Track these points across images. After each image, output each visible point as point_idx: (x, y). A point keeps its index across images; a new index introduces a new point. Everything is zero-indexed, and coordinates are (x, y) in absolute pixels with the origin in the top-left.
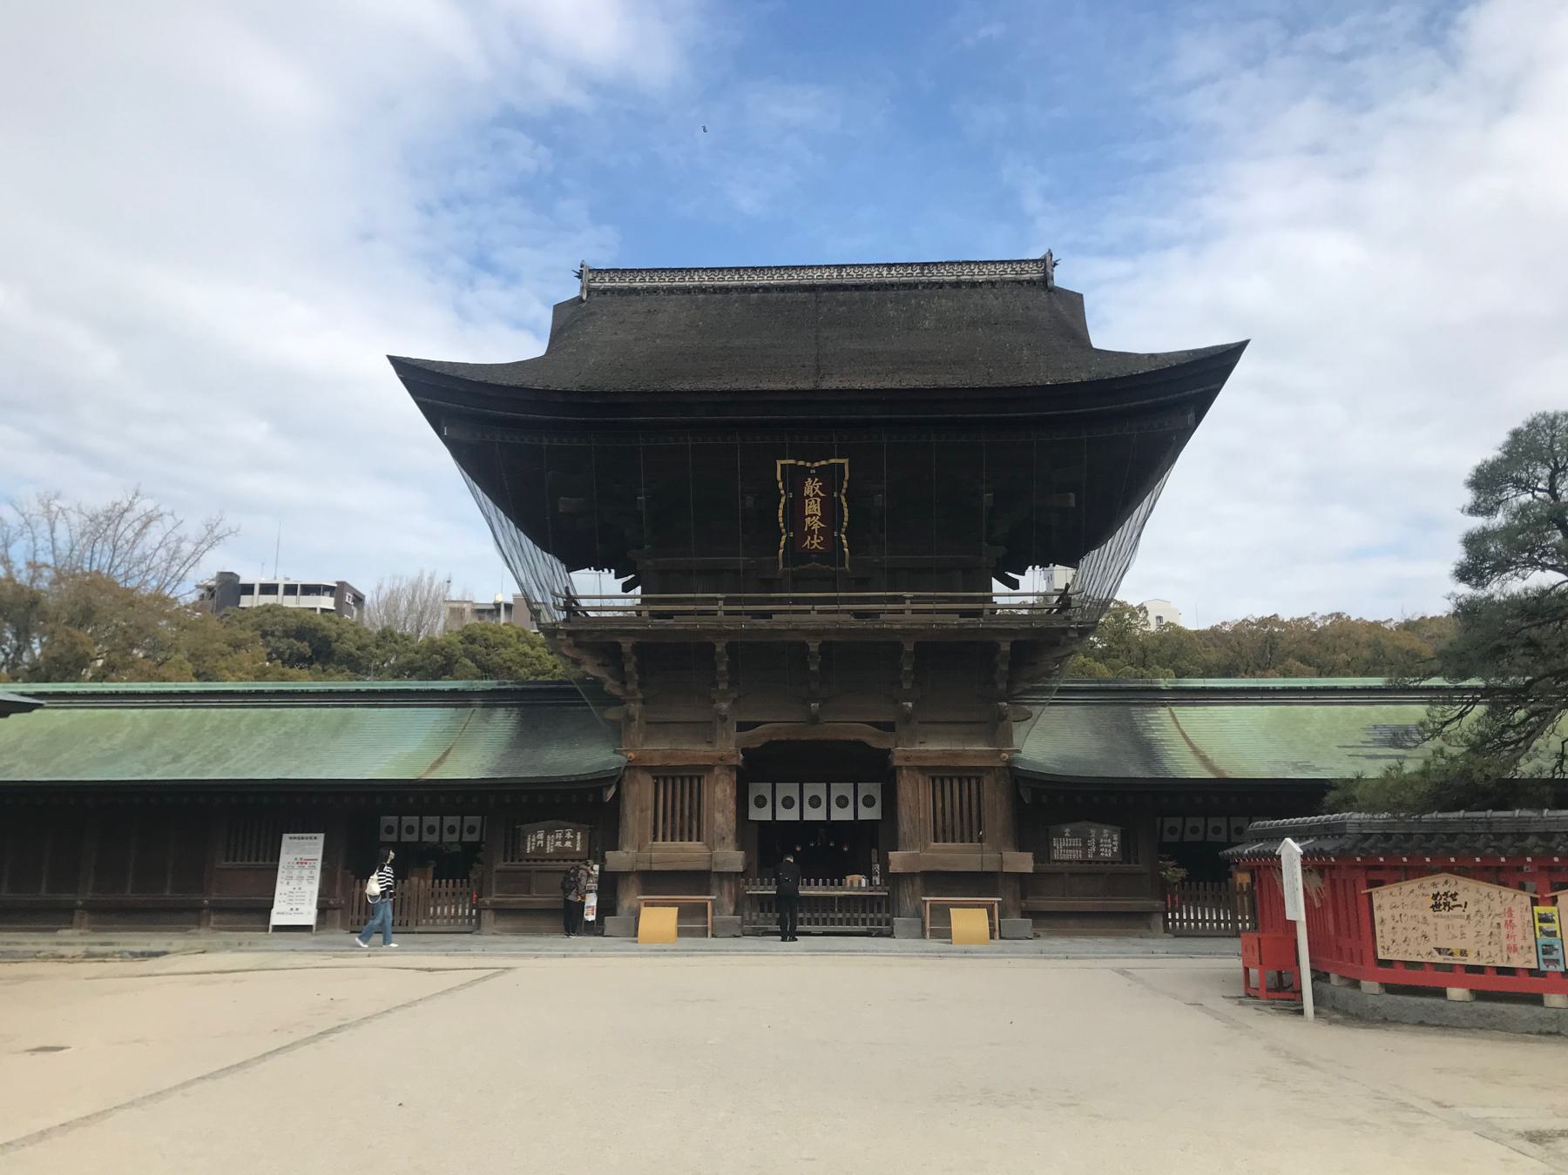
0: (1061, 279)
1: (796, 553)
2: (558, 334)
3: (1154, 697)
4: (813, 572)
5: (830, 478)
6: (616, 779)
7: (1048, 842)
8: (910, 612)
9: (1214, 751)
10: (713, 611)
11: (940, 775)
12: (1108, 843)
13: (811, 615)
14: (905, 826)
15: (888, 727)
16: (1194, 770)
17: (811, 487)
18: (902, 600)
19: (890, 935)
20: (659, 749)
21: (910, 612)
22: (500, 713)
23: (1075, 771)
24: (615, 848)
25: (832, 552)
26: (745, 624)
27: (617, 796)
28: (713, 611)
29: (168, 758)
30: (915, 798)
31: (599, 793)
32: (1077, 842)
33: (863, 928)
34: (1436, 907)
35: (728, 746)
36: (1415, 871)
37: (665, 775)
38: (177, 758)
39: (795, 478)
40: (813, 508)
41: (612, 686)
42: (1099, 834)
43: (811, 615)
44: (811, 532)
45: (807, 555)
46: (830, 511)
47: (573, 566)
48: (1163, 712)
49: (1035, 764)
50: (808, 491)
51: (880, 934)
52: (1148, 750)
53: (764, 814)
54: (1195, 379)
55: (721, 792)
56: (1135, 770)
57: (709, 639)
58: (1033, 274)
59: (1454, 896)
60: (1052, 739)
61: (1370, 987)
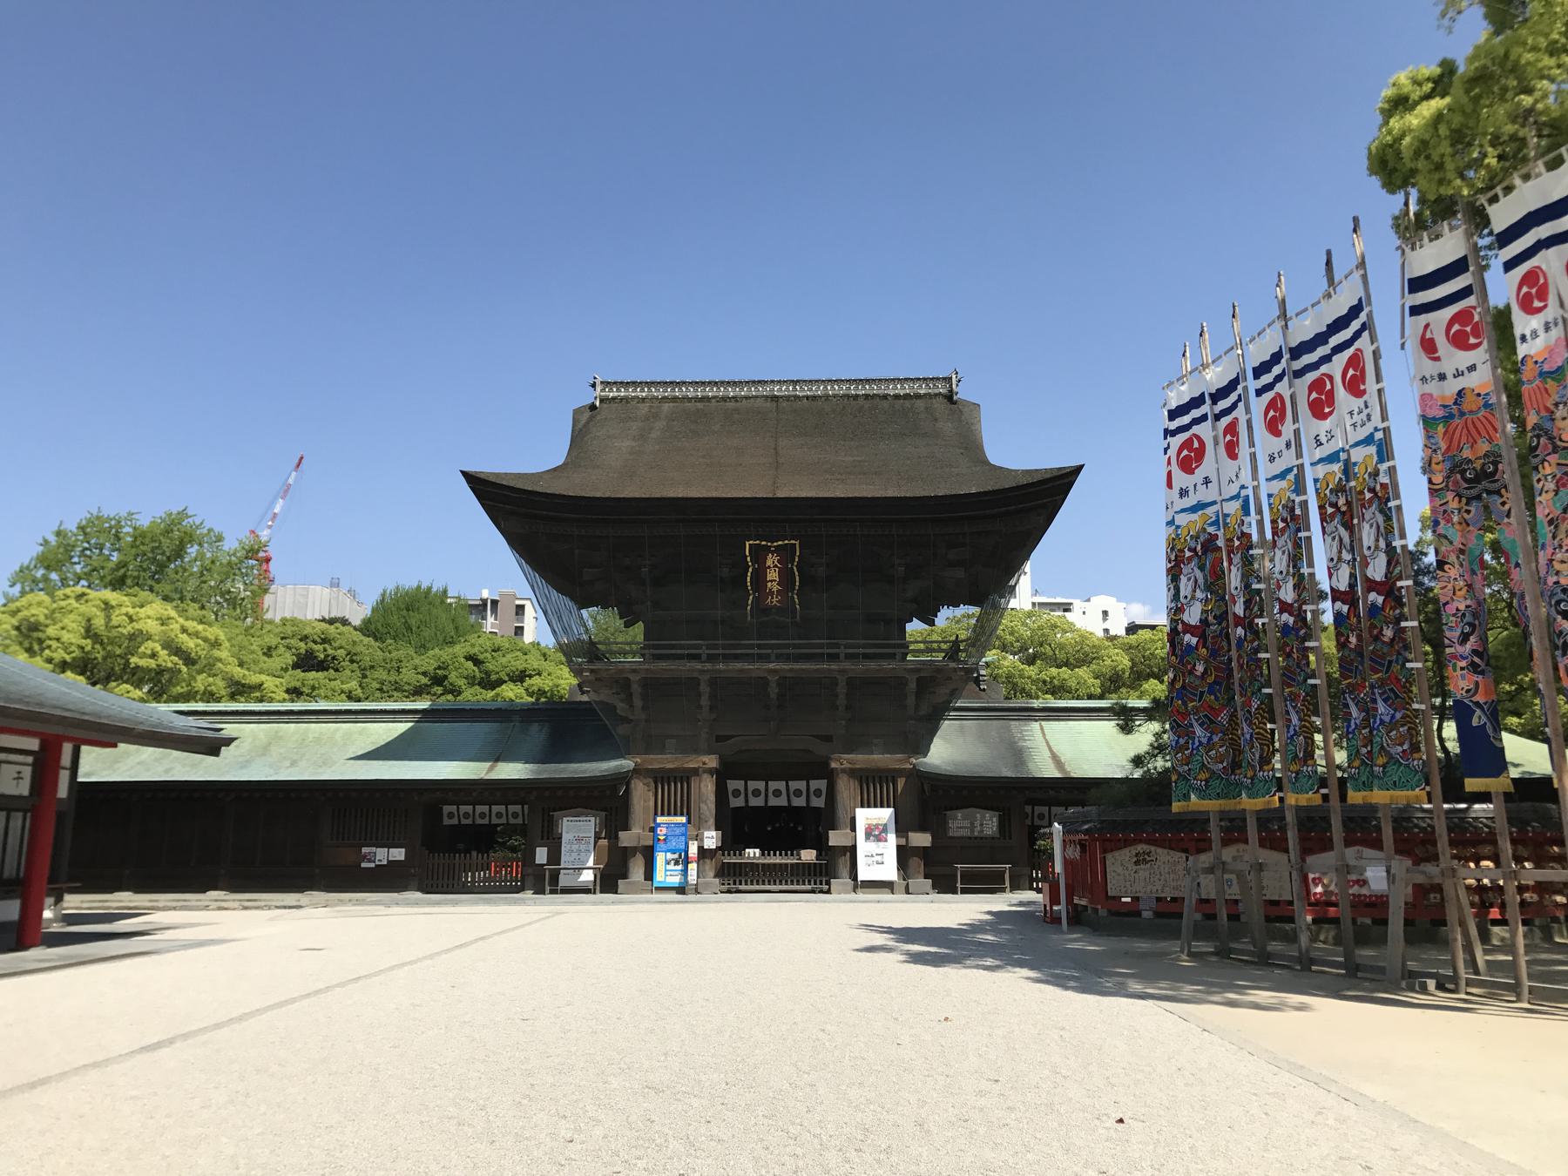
0: (963, 393)
1: (762, 609)
2: (579, 437)
3: (1029, 714)
5: (786, 554)
6: (623, 779)
7: (945, 823)
9: (1066, 754)
12: (988, 823)
15: (828, 739)
16: (1051, 772)
17: (771, 560)
18: (837, 646)
19: (828, 892)
20: (666, 761)
22: (535, 727)
24: (626, 828)
27: (627, 791)
29: (288, 763)
30: (846, 789)
31: (615, 789)
32: (966, 823)
33: (809, 887)
34: (1137, 863)
36: (1127, 843)
38: (294, 763)
39: (759, 554)
40: (773, 575)
41: (621, 707)
42: (983, 817)
44: (771, 593)
45: (766, 610)
46: (786, 578)
47: (583, 604)
48: (1036, 725)
49: (937, 767)
50: (769, 563)
51: (821, 892)
52: (1018, 754)
54: (1050, 491)
56: (1007, 772)
57: (695, 675)
58: (942, 389)
59: (1149, 854)
60: (951, 749)
61: (1102, 912)
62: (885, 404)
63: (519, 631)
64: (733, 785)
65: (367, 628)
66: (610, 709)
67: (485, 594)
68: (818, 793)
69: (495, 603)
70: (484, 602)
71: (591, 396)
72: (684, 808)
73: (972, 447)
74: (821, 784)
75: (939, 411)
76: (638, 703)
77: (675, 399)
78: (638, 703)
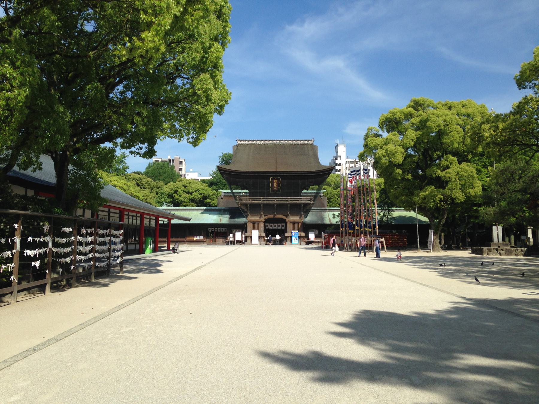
0: (315, 144)
1: (273, 190)
4: (275, 194)
8: (290, 200)
10: (260, 200)
11: (293, 223)
13: (275, 200)
14: (288, 230)
21: (290, 200)
23: (312, 223)
25: (278, 190)
26: (265, 202)
28: (260, 200)
30: (289, 226)
35: (263, 219)
37: (253, 222)
40: (275, 184)
41: (245, 210)
43: (275, 200)
45: (274, 191)
46: (278, 184)
52: (322, 219)
53: (267, 228)
55: (262, 225)
56: (320, 223)
58: (310, 142)
62: (298, 146)
63: (181, 169)
64: (266, 224)
65: (147, 174)
66: (243, 210)
67: (169, 157)
68: (283, 226)
69: (173, 160)
70: (170, 160)
71: (235, 143)
72: (257, 229)
73: (316, 157)
74: (284, 224)
75: (309, 150)
76: (249, 209)
77: (254, 144)
78: (249, 209)
